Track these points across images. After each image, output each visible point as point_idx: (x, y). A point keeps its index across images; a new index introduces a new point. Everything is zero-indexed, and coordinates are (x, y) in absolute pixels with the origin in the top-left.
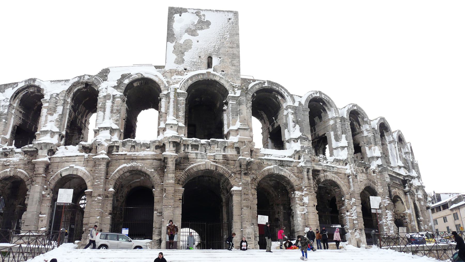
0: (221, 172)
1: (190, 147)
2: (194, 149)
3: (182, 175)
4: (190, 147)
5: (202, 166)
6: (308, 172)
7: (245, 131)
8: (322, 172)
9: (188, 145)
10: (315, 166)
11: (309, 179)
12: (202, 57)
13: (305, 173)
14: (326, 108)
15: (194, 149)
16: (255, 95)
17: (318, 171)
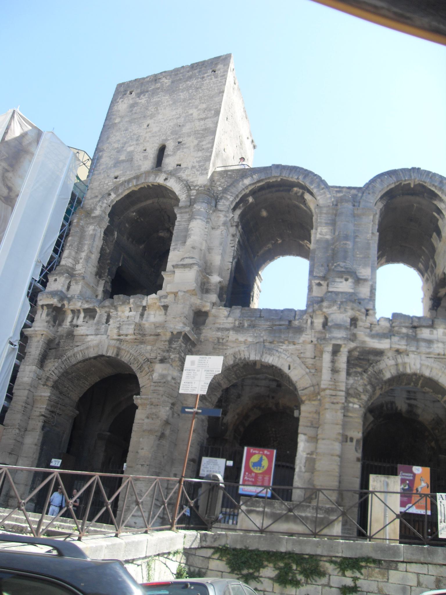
0: (125, 358)
1: (82, 315)
2: (88, 317)
3: (53, 367)
4: (82, 315)
5: (92, 350)
6: (336, 350)
7: (187, 270)
8: (390, 354)
9: (79, 311)
10: (367, 339)
11: (334, 371)
12: (148, 149)
13: (327, 357)
14: (441, 206)
15: (88, 317)
16: (251, 200)
17: (380, 353)
